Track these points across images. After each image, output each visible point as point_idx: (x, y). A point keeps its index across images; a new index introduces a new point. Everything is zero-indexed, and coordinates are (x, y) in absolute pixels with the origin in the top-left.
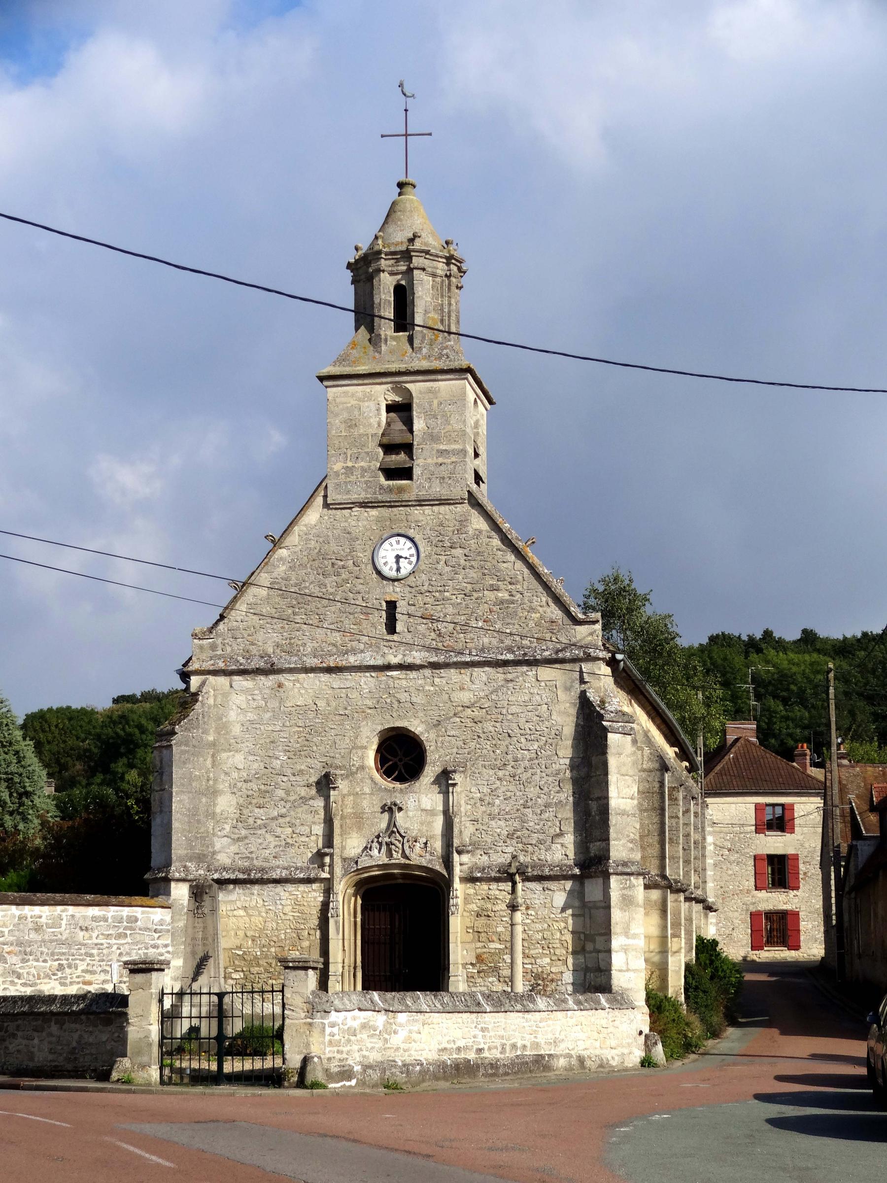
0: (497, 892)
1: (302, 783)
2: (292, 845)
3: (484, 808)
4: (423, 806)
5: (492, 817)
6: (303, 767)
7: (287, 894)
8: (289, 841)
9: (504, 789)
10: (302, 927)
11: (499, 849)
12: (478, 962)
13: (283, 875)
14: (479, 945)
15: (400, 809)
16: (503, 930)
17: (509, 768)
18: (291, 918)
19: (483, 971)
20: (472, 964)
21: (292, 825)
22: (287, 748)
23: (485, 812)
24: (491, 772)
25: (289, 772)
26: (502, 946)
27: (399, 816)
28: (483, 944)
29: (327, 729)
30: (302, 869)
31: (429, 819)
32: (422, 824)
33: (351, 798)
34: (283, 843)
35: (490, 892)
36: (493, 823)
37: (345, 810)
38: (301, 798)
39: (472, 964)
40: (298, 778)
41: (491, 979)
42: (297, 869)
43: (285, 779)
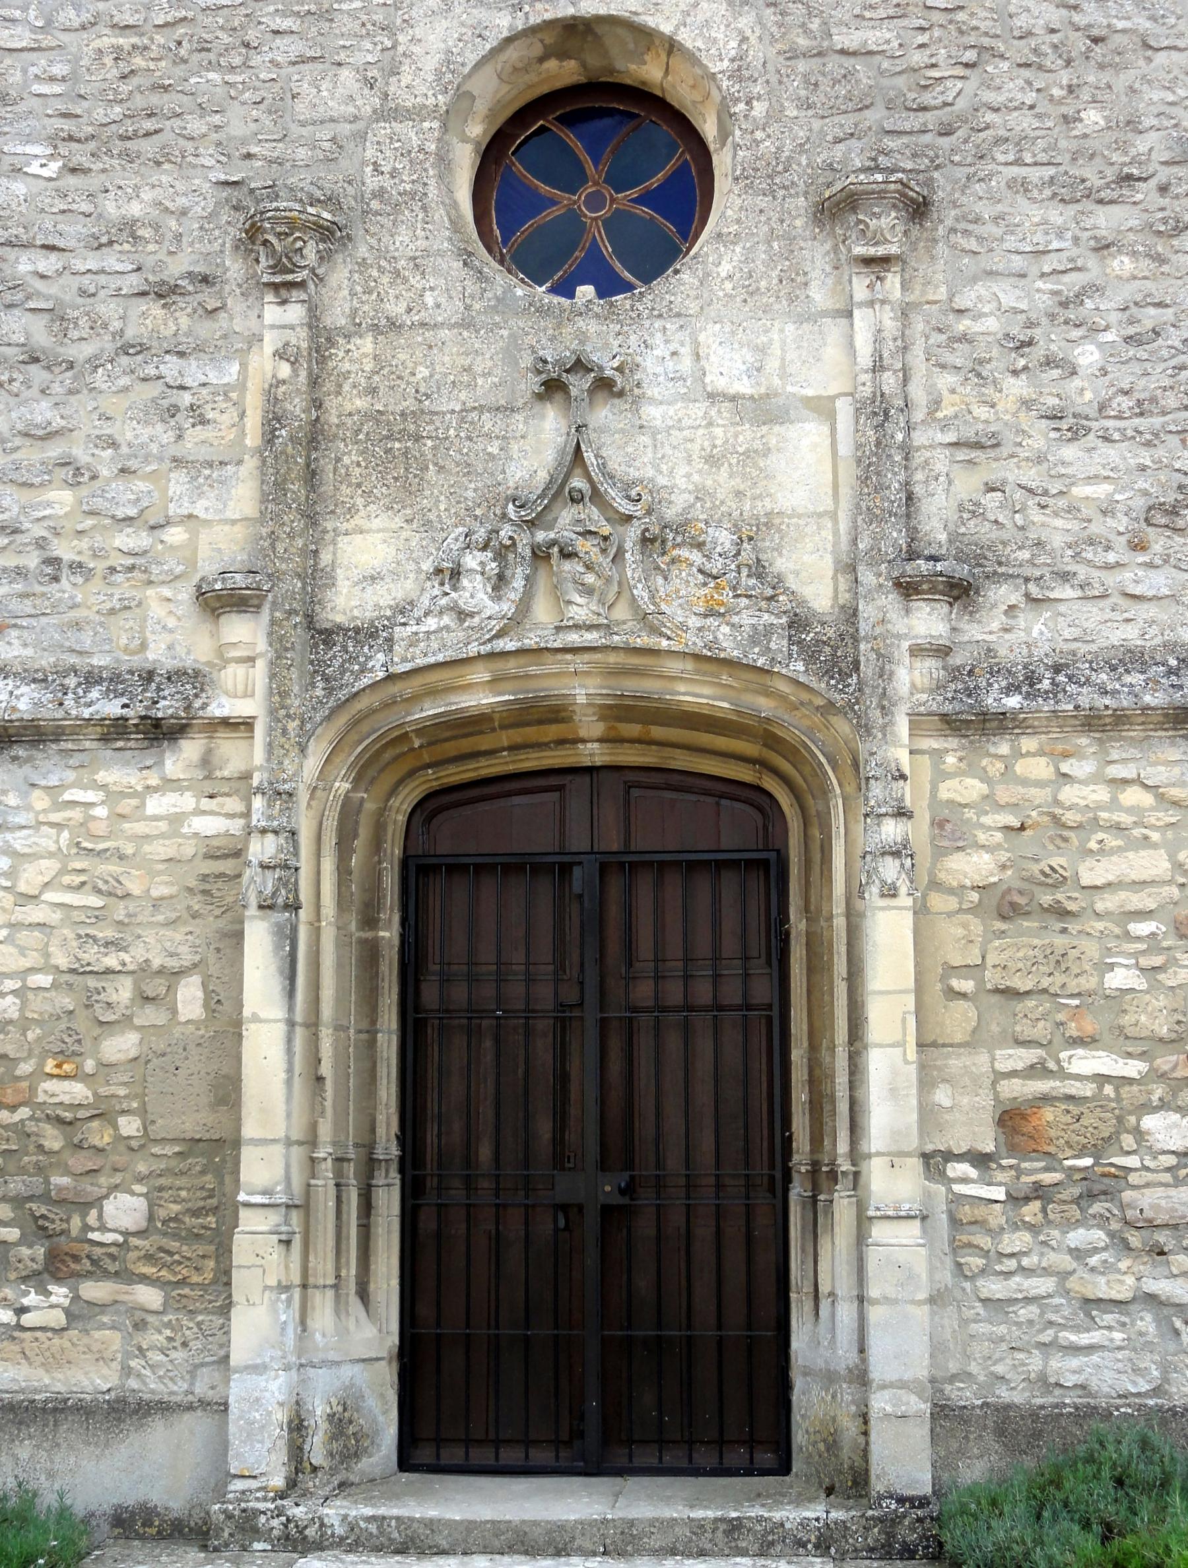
0: (1101, 794)
1: (133, 282)
2: (77, 567)
3: (1017, 387)
4: (716, 381)
5: (1069, 424)
6: (135, 209)
7: (40, 800)
8: (64, 550)
9: (1129, 292)
10: (111, 961)
11: (1112, 579)
12: (1013, 1149)
13: (23, 705)
14: (1016, 1058)
15: (604, 386)
16: (1136, 981)
17: (1144, 192)
18: (55, 917)
19: (1039, 1192)
20: (981, 1160)
21: (75, 473)
22: (67, 125)
23: (1027, 404)
24: (1057, 215)
25: (73, 232)
26: (1133, 1068)
27: (604, 415)
28: (1029, 1056)
29: (252, 35)
30: (116, 678)
31: (747, 436)
32: (712, 460)
33: (367, 344)
34: (32, 561)
35: (1068, 794)
36: (1070, 452)
37: (331, 403)
38: (125, 350)
39: (981, 1160)
40: (111, 260)
41: (1078, 1237)
42: (91, 679)
43: (48, 263)
